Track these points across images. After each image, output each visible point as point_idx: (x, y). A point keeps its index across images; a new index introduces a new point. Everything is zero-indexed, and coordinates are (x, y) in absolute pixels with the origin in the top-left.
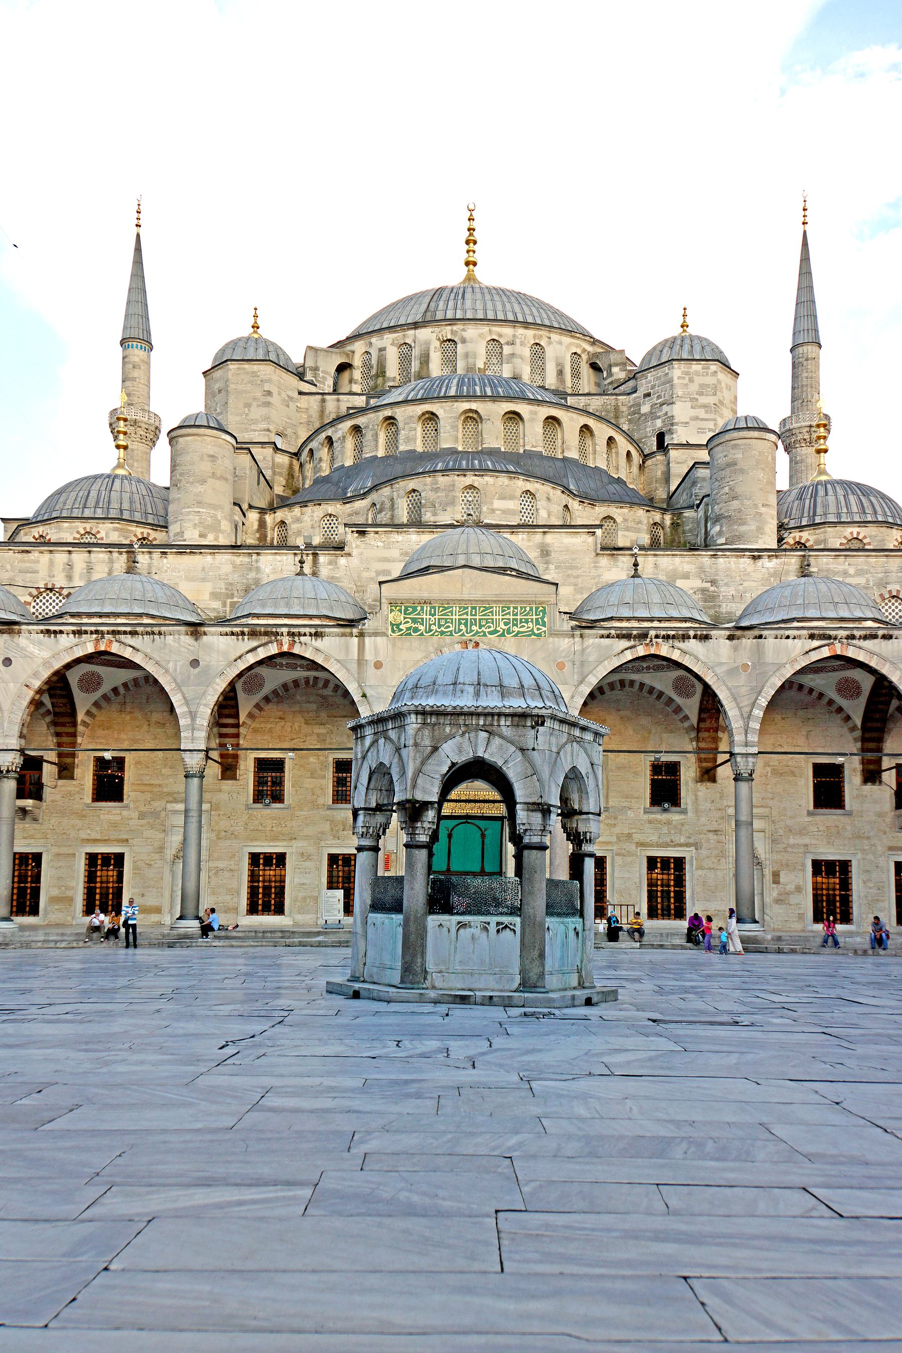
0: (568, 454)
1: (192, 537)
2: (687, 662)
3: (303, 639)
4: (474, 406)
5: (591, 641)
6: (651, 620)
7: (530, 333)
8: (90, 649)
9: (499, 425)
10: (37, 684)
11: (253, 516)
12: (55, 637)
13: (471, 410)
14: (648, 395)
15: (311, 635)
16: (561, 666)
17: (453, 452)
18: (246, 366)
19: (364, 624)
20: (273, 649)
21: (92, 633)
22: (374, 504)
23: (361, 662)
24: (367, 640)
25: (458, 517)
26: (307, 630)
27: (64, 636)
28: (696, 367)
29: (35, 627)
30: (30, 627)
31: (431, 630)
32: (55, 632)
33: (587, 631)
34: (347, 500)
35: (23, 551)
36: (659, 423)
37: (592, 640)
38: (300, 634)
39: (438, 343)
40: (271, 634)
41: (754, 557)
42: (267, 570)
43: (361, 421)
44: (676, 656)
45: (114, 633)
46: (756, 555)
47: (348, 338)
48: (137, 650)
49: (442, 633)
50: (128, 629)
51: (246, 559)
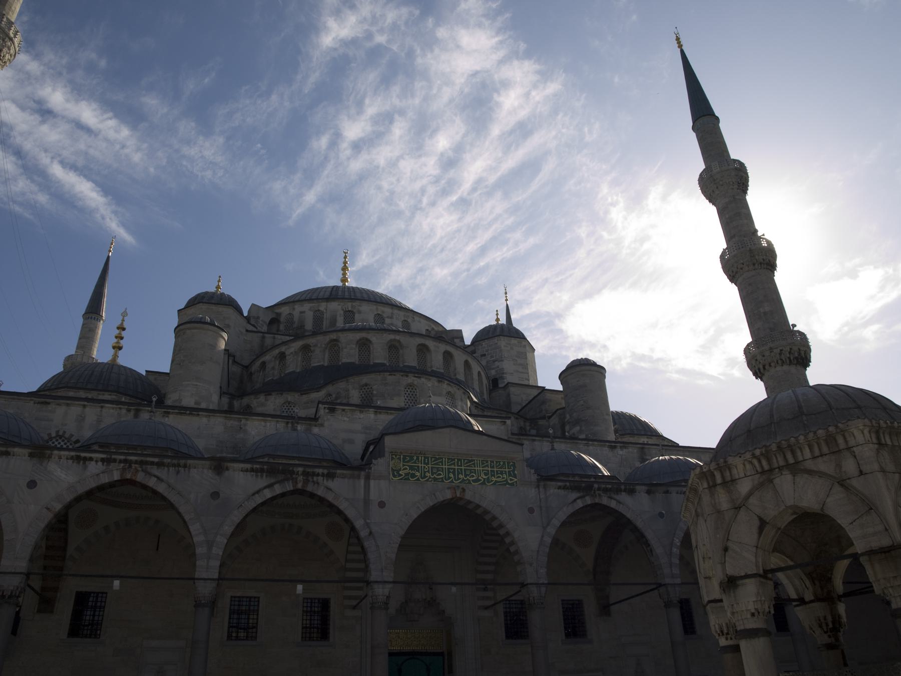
0: (458, 377)
1: (188, 401)
2: (621, 509)
3: (315, 479)
4: (398, 337)
5: (552, 491)
6: (590, 476)
7: (402, 313)
8: (116, 476)
9: (414, 351)
10: (58, 507)
11: (225, 400)
12: (84, 463)
13: (395, 340)
14: (484, 355)
15: (323, 475)
16: (531, 510)
17: (383, 365)
18: (214, 307)
19: (370, 468)
20: (289, 487)
21: (120, 461)
22: (330, 395)
23: (367, 501)
24: (372, 483)
25: (402, 405)
26: (320, 471)
27: (93, 463)
28: (514, 341)
29: (66, 453)
30: (62, 453)
31: (425, 477)
32: (85, 459)
33: (549, 483)
34: (304, 392)
35: (42, 403)
36: (493, 372)
37: (553, 490)
38: (314, 474)
39: (342, 312)
40: (287, 473)
41: (613, 448)
42: (253, 433)
43: (311, 341)
44: (613, 504)
45: (142, 463)
46: (612, 446)
47: (275, 305)
48: (162, 480)
49: (435, 479)
50: (156, 460)
51: (236, 423)
